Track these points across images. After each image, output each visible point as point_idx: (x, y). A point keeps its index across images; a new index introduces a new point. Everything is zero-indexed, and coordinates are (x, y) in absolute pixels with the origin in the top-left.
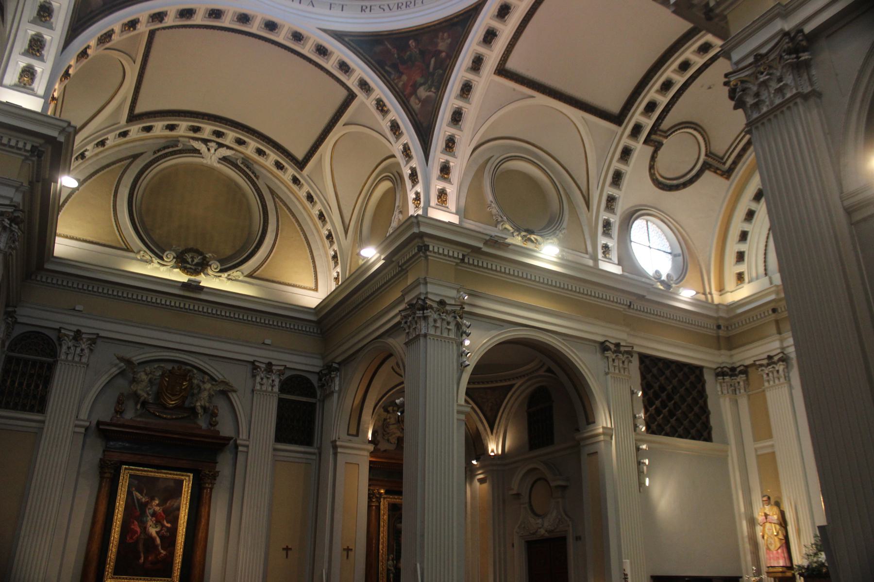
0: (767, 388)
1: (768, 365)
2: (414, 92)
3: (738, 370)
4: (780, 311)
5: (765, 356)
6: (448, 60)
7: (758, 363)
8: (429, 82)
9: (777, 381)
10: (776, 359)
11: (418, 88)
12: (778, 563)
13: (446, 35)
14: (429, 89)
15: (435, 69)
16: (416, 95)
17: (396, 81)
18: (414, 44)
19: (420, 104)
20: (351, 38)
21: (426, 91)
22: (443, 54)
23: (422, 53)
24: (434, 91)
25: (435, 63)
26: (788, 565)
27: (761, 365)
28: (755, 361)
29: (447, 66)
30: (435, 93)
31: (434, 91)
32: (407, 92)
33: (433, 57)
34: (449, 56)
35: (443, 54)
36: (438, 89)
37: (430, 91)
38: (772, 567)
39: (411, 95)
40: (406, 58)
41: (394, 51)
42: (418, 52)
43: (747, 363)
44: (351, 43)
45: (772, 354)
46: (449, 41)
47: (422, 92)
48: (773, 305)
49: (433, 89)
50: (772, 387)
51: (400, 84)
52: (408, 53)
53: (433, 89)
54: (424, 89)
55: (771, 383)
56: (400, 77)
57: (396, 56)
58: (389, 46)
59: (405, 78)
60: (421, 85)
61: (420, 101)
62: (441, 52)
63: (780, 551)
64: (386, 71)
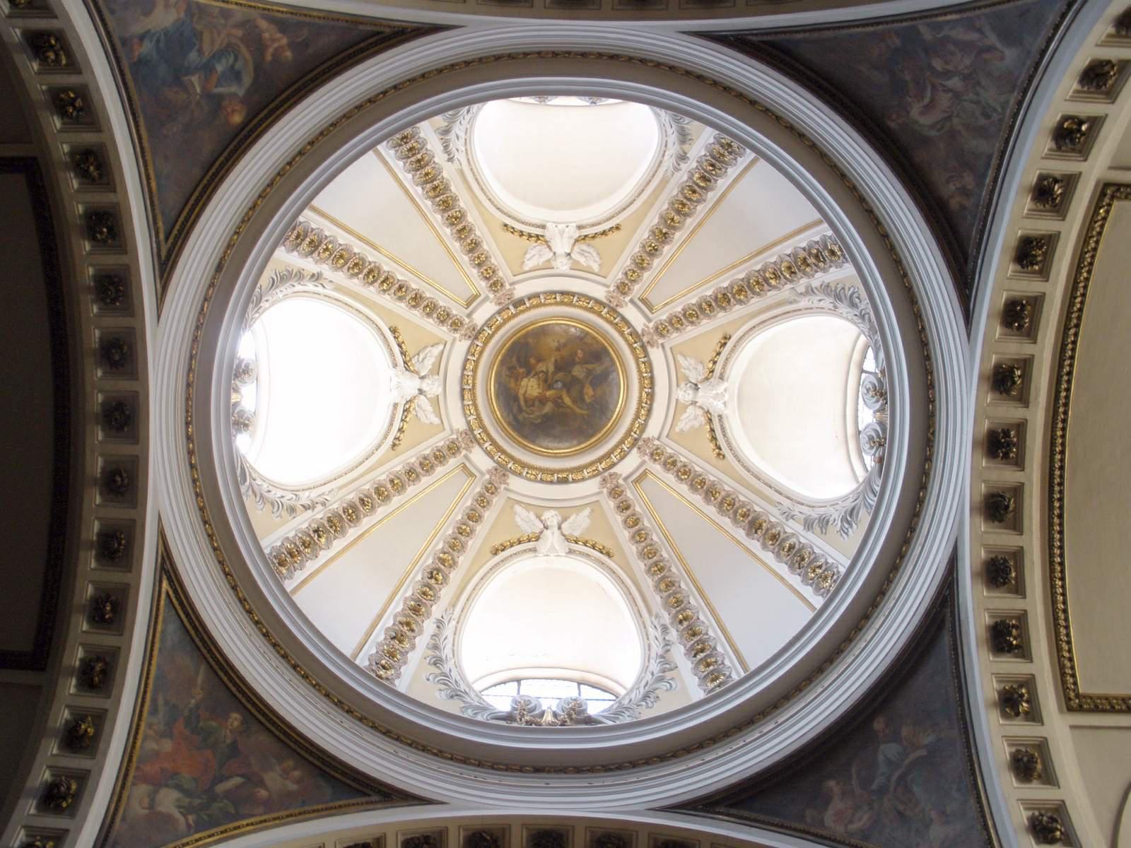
2: (158, 783)
6: (261, 809)
8: (197, 802)
11: (167, 786)
13: (297, 773)
14: (185, 811)
15: (228, 794)
16: (156, 792)
17: (151, 732)
18: (236, 724)
19: (146, 811)
20: (171, 593)
21: (179, 807)
22: (263, 793)
23: (234, 749)
24: (191, 822)
25: (238, 787)
29: (253, 816)
30: (189, 826)
31: (191, 822)
32: (148, 769)
33: (242, 776)
34: (269, 805)
35: (263, 793)
36: (200, 826)
37: (184, 815)
39: (145, 779)
40: (201, 724)
41: (198, 694)
42: (228, 741)
44: (163, 596)
46: (292, 787)
47: (168, 800)
49: (191, 818)
51: (154, 746)
52: (214, 724)
53: (191, 818)
54: (178, 800)
56: (163, 735)
57: (193, 701)
58: (200, 679)
59: (167, 745)
60: (179, 787)
61: (151, 807)
62: (261, 783)
64: (154, 701)
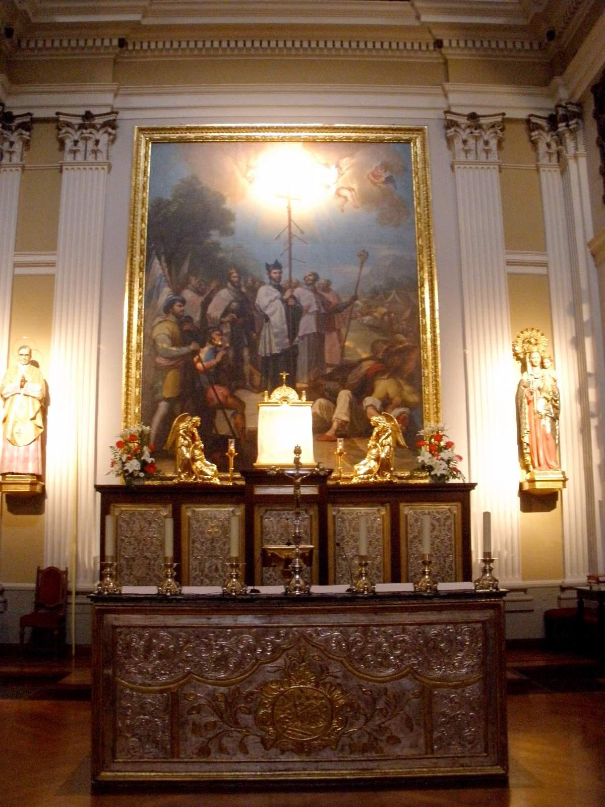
0: (70, 164)
1: (81, 127)
3: (18, 121)
4: (130, 47)
5: (82, 112)
7: (62, 118)
9: (91, 158)
10: (98, 121)
12: (26, 467)
26: (40, 473)
27: (68, 125)
28: (58, 114)
38: (13, 474)
43: (38, 114)
45: (95, 111)
48: (122, 33)
50: (79, 164)
55: (80, 157)
63: (32, 446)
